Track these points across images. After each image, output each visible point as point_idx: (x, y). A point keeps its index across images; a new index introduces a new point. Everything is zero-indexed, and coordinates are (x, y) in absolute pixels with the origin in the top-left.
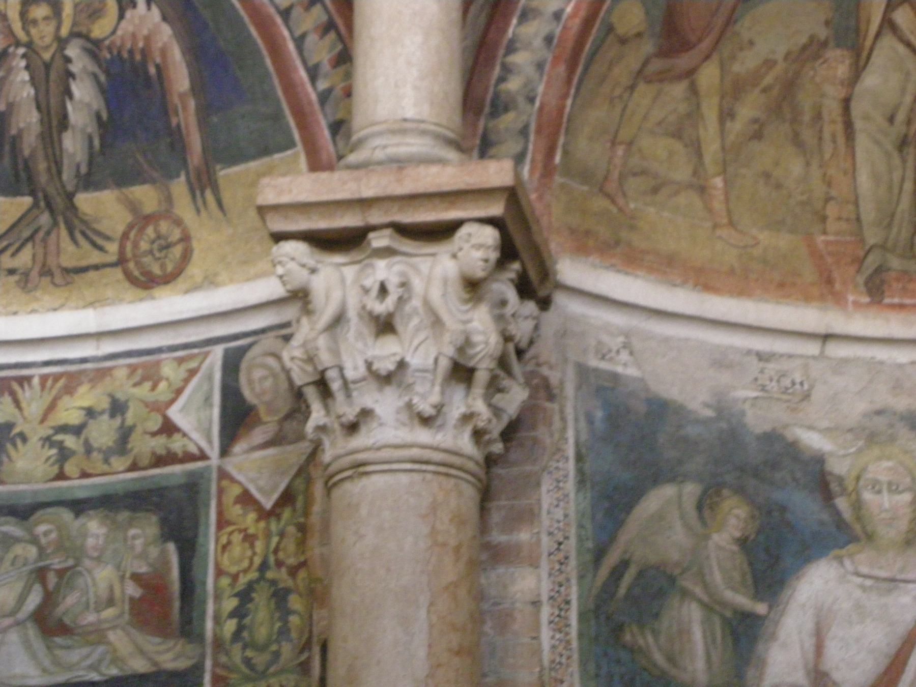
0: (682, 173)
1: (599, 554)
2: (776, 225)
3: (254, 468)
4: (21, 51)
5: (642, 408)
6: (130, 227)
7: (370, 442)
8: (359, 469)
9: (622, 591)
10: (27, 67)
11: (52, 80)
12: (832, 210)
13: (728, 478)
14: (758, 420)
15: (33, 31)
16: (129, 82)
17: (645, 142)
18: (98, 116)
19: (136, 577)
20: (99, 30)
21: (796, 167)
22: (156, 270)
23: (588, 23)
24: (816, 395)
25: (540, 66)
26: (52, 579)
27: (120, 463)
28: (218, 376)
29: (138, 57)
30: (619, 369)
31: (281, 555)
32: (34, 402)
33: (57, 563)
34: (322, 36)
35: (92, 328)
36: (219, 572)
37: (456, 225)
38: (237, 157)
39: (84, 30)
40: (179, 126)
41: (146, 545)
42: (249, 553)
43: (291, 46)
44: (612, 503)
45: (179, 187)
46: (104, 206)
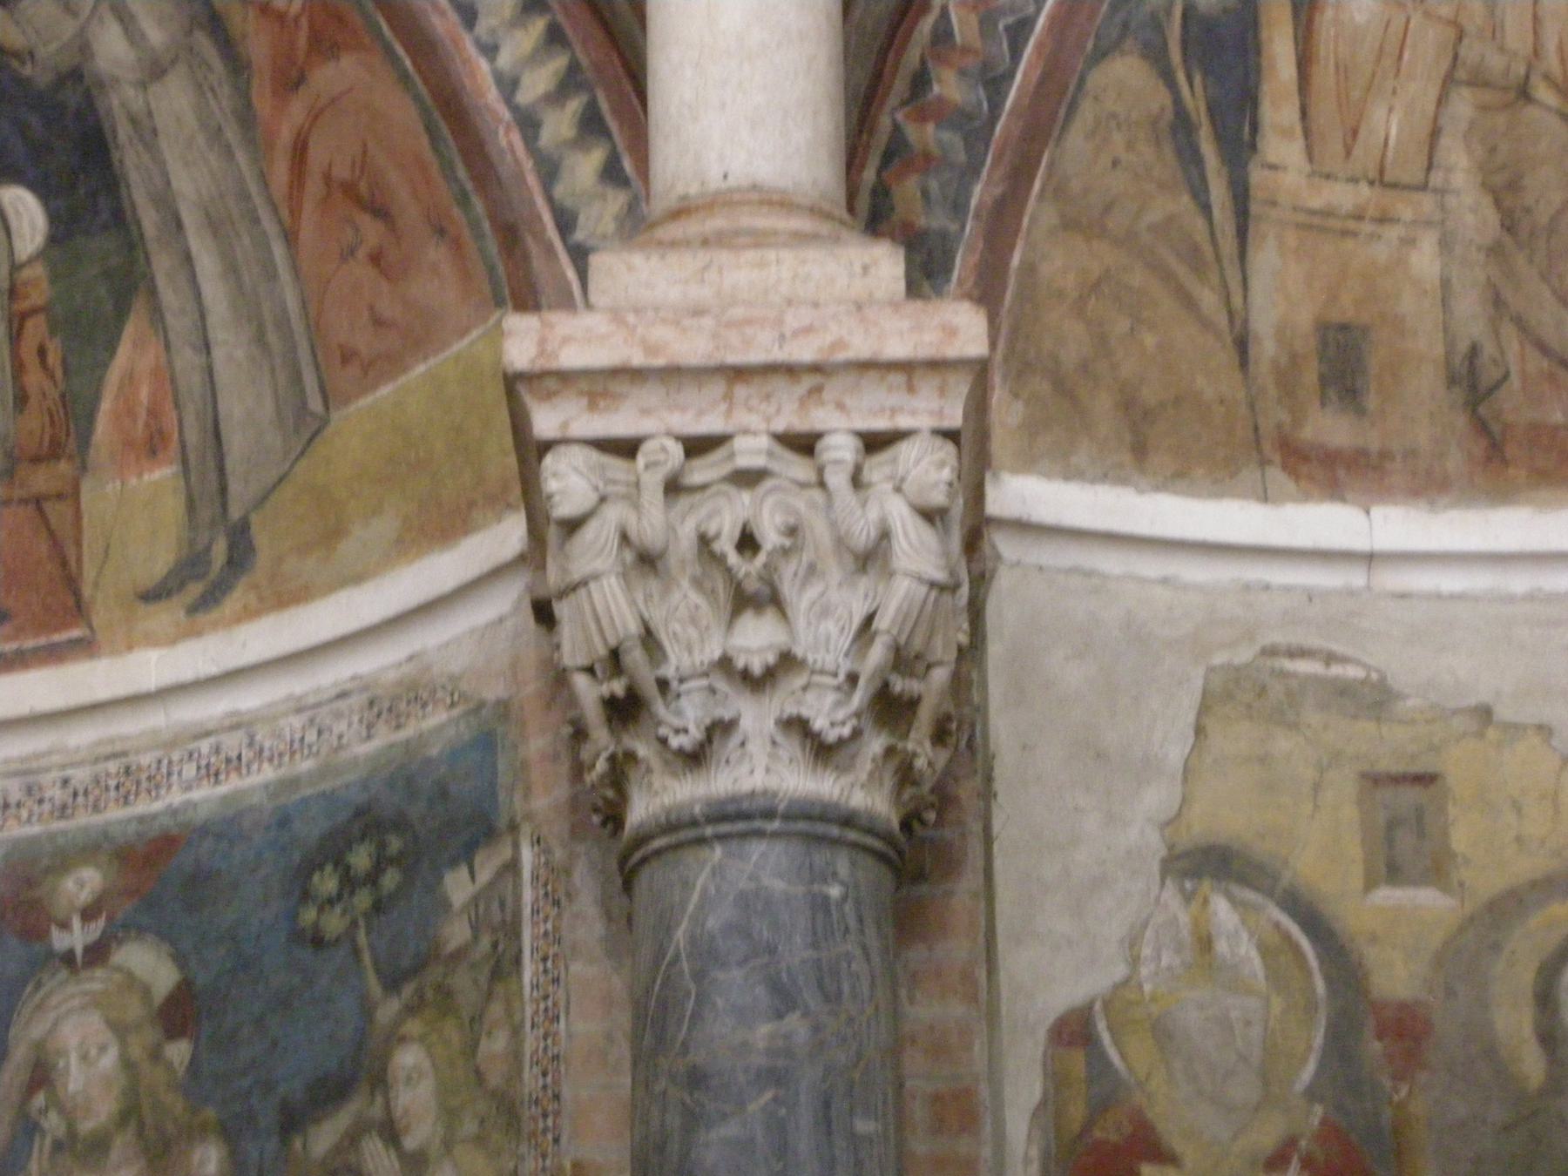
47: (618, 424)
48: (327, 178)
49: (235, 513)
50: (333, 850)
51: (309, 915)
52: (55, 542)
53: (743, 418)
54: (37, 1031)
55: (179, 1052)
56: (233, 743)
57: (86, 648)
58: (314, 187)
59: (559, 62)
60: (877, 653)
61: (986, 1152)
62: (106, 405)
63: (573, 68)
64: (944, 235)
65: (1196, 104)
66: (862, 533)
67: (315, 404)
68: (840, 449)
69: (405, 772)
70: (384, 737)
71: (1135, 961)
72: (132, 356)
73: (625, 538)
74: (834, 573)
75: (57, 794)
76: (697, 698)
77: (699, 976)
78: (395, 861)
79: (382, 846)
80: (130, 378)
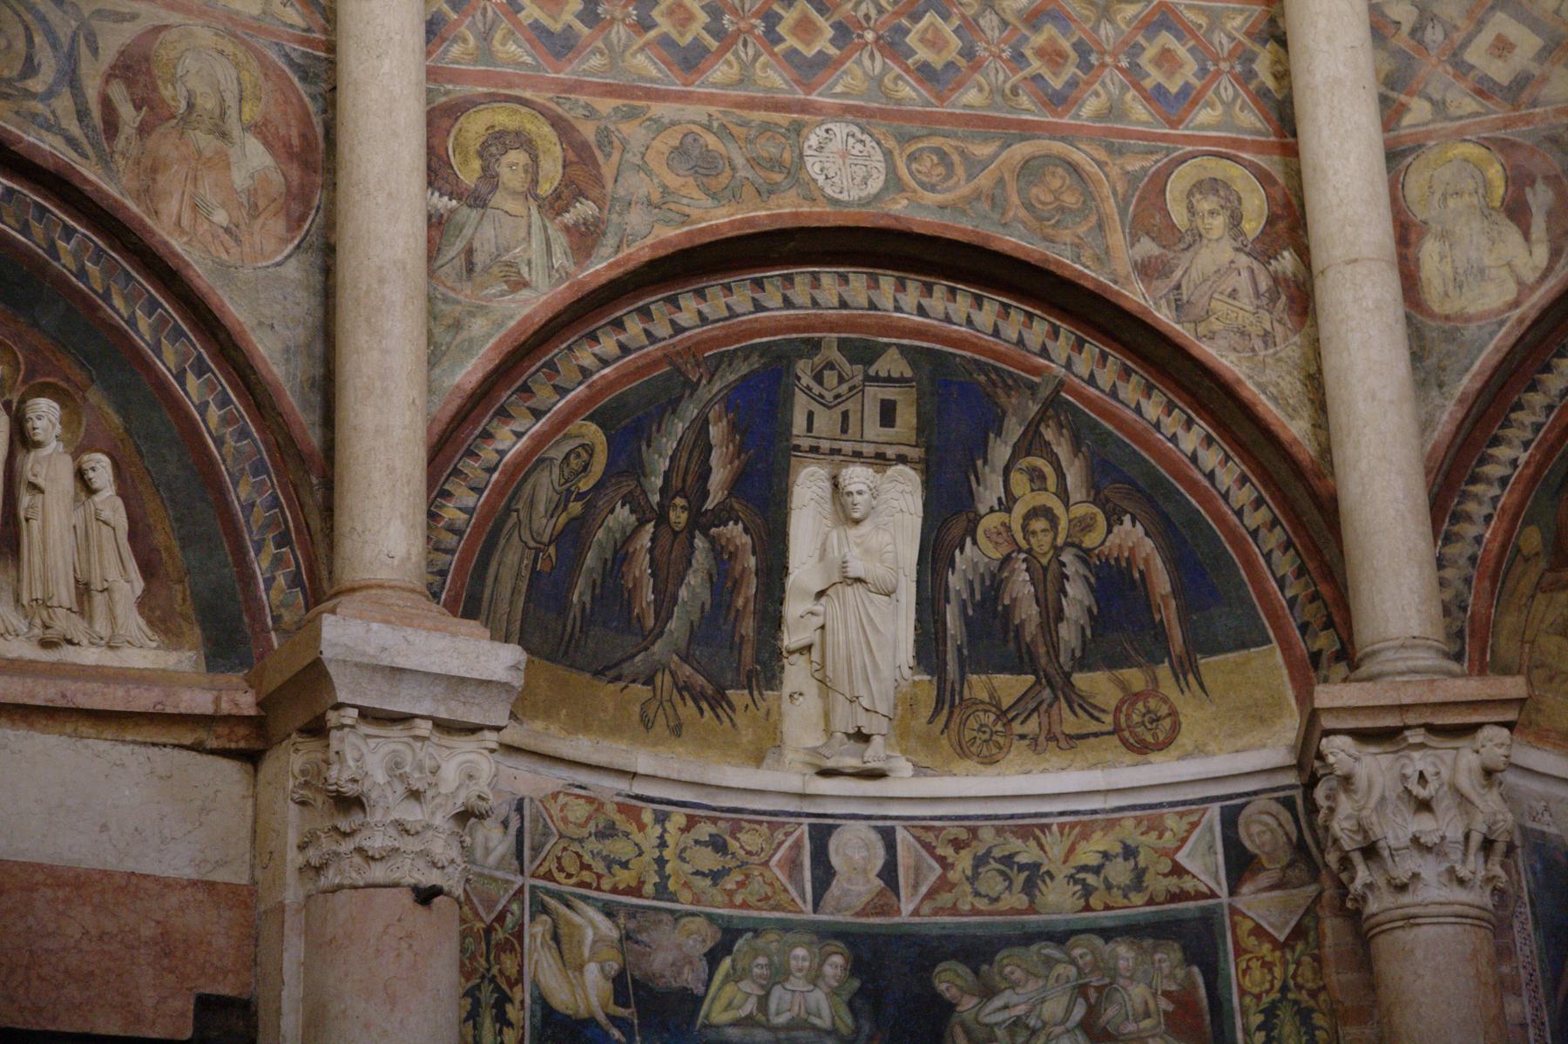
4: (1023, 556)
6: (1122, 702)
7: (1419, 899)
8: (1410, 920)
10: (1027, 570)
11: (1049, 582)
15: (1033, 540)
16: (1116, 585)
17: (1542, 639)
18: (1089, 610)
19: (1167, 994)
20: (1090, 541)
22: (1149, 739)
23: (1504, 547)
25: (1467, 581)
26: (1093, 995)
27: (1138, 899)
29: (1124, 564)
30: (1545, 828)
31: (1300, 980)
32: (1056, 847)
33: (1095, 981)
34: (1284, 553)
35: (1103, 786)
36: (1243, 993)
37: (1477, 727)
39: (1077, 541)
41: (1173, 968)
42: (1269, 977)
43: (1262, 561)
45: (1164, 671)
46: (1097, 684)
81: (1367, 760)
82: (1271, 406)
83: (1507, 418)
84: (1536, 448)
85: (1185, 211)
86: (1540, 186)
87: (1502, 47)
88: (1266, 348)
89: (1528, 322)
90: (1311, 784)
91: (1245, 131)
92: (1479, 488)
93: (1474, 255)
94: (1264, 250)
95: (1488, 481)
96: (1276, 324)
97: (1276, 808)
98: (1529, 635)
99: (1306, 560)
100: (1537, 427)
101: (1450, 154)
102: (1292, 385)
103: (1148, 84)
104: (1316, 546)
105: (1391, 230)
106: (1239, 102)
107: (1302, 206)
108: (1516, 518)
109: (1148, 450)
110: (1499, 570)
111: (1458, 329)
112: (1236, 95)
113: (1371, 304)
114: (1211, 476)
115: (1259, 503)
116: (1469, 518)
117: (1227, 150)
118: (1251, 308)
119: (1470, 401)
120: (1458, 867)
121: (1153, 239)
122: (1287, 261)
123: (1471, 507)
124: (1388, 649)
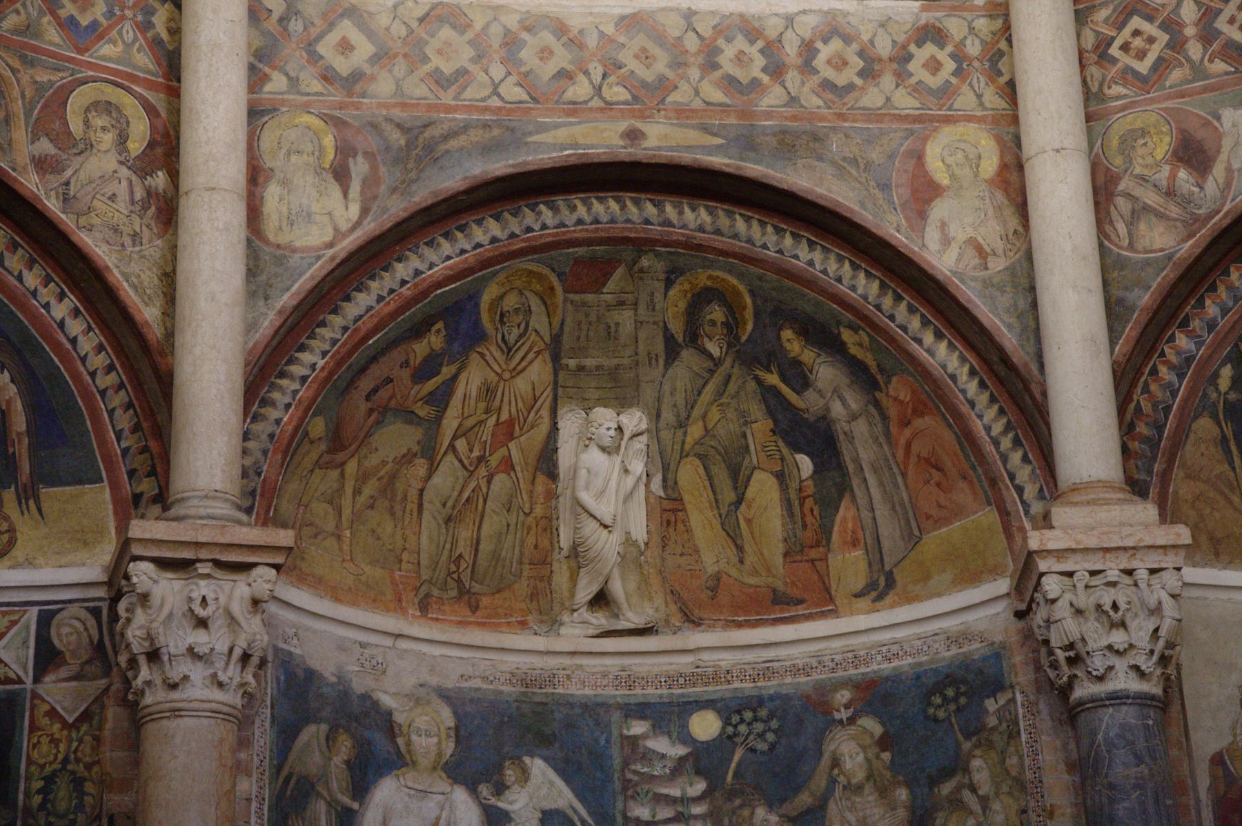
0: (330, 526)
1: (279, 768)
2: (373, 562)
3: (60, 693)
5: (301, 674)
7: (185, 696)
8: (176, 713)
9: (289, 792)
12: (405, 556)
13: (343, 722)
14: (360, 685)
17: (314, 505)
21: (389, 526)
24: (390, 672)
25: (265, 452)
28: (33, 627)
30: (292, 649)
36: (30, 762)
37: (252, 566)
38: (55, 480)
40: (14, 453)
42: (54, 751)
43: (106, 416)
44: (287, 734)
47: (1068, 567)
48: (918, 456)
49: (887, 568)
50: (938, 688)
51: (932, 711)
52: (821, 577)
53: (1109, 564)
54: (832, 747)
55: (886, 756)
56: (895, 649)
57: (834, 613)
58: (913, 459)
59: (1004, 420)
60: (1161, 643)
61: (1192, 802)
62: (836, 529)
63: (1009, 422)
64: (1145, 481)
65: (1229, 433)
66: (1153, 603)
67: (917, 533)
68: (1142, 574)
69: (965, 664)
70: (954, 651)
71: (1235, 735)
72: (845, 512)
73: (1071, 604)
74: (1142, 616)
75: (831, 665)
76: (1100, 658)
77: (1109, 752)
78: (963, 694)
79: (958, 688)
80: (844, 520)
81: (163, 583)
82: (131, 292)
83: (313, 332)
84: (331, 358)
85: (81, 124)
86: (360, 158)
87: (345, 47)
88: (134, 245)
89: (338, 261)
90: (115, 600)
91: (139, 69)
92: (284, 382)
93: (305, 201)
94: (143, 166)
95: (291, 377)
96: (144, 228)
97: (84, 614)
98: (304, 501)
99: (142, 419)
100: (334, 342)
101: (297, 121)
102: (150, 278)
103: (63, 13)
104: (151, 410)
105: (244, 170)
106: (137, 45)
107: (178, 138)
108: (309, 409)
109: (24, 313)
110: (290, 447)
111: (285, 257)
112: (135, 39)
113: (221, 225)
114: (74, 341)
115: (110, 368)
116: (273, 404)
117: (123, 81)
118: (126, 212)
119: (287, 313)
120: (220, 673)
121: (51, 141)
122: (160, 180)
123: (276, 395)
124: (193, 497)
